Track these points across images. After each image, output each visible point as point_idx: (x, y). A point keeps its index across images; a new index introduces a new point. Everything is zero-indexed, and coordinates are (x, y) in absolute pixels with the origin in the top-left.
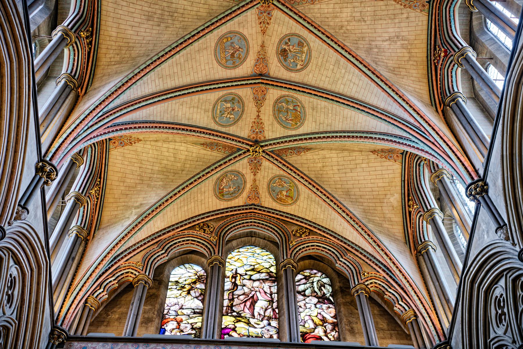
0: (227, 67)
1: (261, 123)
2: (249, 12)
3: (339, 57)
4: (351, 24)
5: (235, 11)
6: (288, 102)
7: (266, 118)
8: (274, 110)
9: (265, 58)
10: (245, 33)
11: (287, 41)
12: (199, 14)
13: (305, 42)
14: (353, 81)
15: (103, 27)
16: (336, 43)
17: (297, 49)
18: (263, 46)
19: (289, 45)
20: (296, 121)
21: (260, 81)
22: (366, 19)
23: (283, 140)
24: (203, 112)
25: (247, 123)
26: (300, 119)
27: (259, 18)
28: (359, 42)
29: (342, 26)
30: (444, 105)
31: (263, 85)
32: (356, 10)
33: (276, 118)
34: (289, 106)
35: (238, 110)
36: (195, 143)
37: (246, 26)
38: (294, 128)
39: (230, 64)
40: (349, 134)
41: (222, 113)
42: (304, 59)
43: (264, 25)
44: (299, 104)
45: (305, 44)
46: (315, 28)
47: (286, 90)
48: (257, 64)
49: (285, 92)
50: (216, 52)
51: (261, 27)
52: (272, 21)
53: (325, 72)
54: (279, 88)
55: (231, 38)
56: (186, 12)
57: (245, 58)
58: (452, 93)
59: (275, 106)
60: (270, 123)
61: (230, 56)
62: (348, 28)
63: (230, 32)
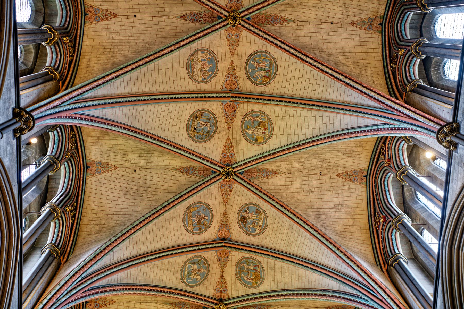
0: (193, 233)
1: (225, 283)
2: (213, 186)
3: (292, 222)
4: (301, 195)
5: (201, 185)
6: (249, 263)
7: (230, 278)
8: (236, 271)
9: (227, 224)
10: (210, 203)
11: (246, 209)
12: (170, 188)
13: (262, 210)
14: (306, 243)
15: (86, 202)
16: (288, 211)
17: (255, 216)
18: (225, 214)
19: (248, 213)
20: (256, 280)
21: (223, 244)
22: (313, 190)
23: (245, 298)
24: (172, 274)
25: (212, 283)
26: (259, 278)
27: (221, 191)
28: (309, 210)
29: (293, 197)
30: (388, 265)
31: (226, 248)
32: (304, 182)
33: (238, 277)
34: (249, 267)
35: (204, 271)
36: (165, 303)
37: (211, 197)
38: (255, 287)
39: (196, 230)
40: (305, 292)
41: (189, 274)
42: (261, 225)
43: (226, 197)
44: (258, 264)
45: (262, 212)
46: (270, 198)
47: (247, 252)
48: (221, 229)
49: (245, 254)
50: (184, 221)
51: (223, 198)
52: (232, 193)
53: (280, 236)
54: (240, 251)
55: (197, 208)
56: (158, 187)
57: (209, 225)
58: (394, 254)
59: (237, 267)
60: (233, 282)
61: (196, 223)
62: (299, 197)
63: (197, 203)
